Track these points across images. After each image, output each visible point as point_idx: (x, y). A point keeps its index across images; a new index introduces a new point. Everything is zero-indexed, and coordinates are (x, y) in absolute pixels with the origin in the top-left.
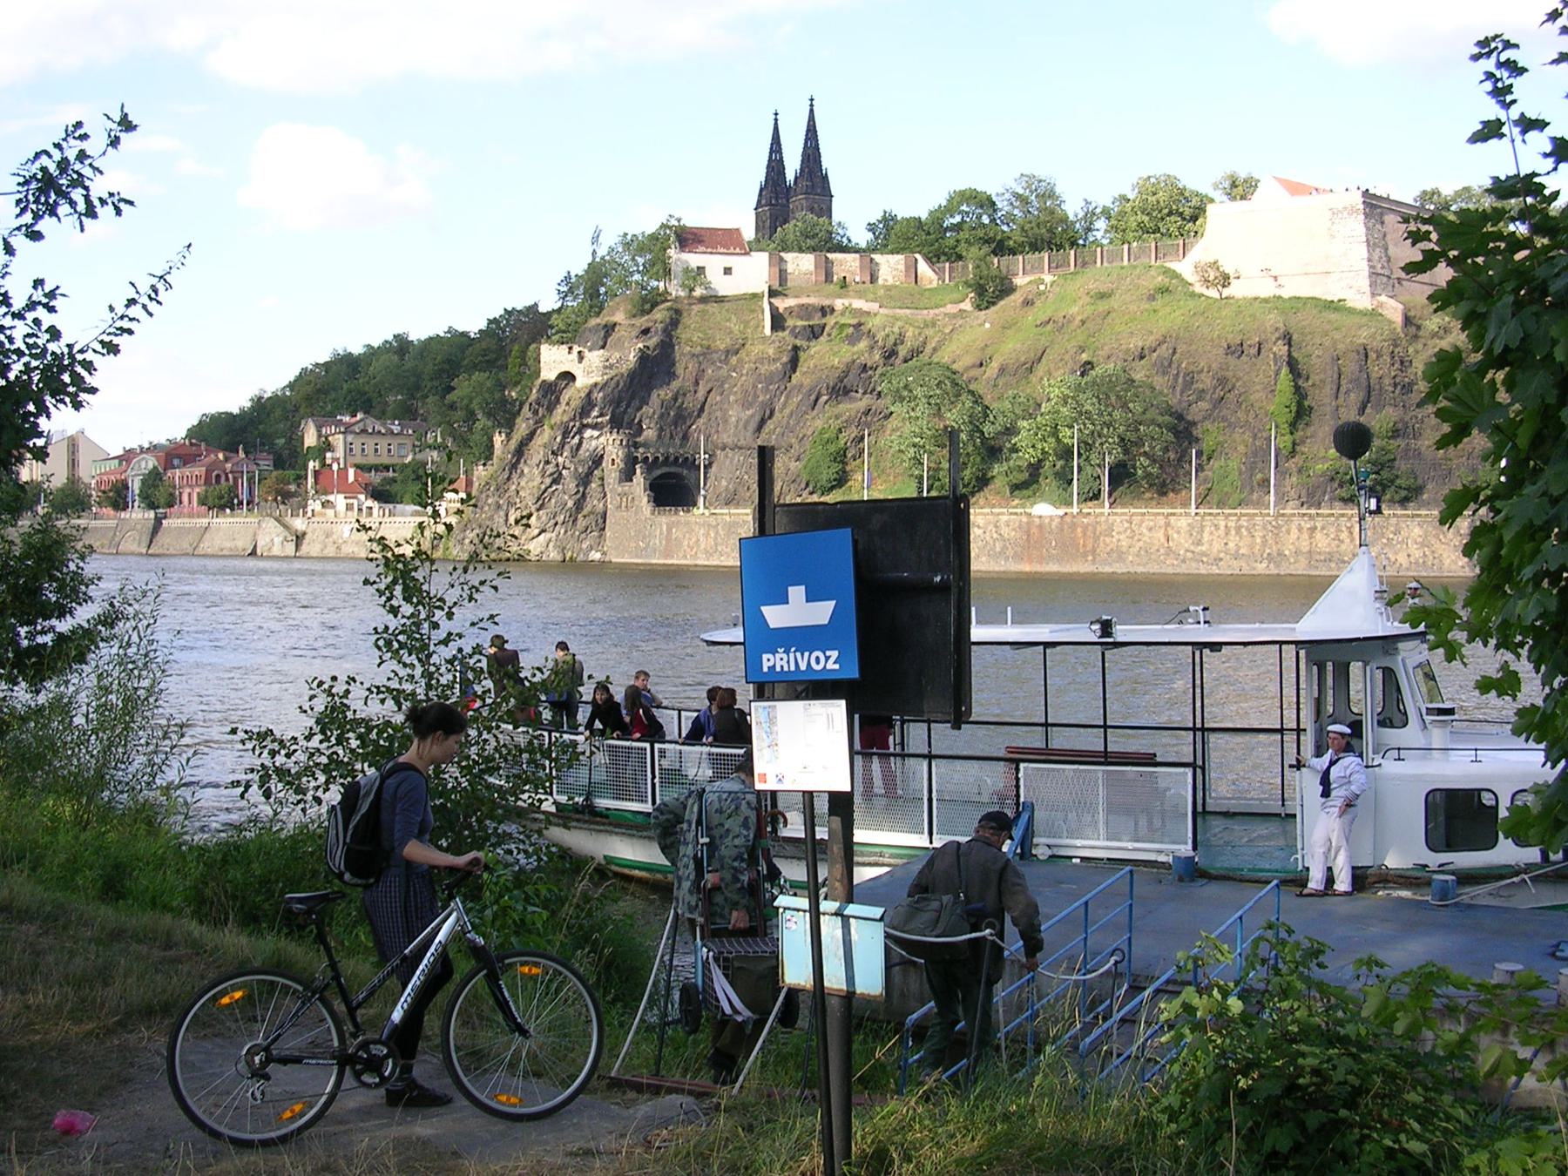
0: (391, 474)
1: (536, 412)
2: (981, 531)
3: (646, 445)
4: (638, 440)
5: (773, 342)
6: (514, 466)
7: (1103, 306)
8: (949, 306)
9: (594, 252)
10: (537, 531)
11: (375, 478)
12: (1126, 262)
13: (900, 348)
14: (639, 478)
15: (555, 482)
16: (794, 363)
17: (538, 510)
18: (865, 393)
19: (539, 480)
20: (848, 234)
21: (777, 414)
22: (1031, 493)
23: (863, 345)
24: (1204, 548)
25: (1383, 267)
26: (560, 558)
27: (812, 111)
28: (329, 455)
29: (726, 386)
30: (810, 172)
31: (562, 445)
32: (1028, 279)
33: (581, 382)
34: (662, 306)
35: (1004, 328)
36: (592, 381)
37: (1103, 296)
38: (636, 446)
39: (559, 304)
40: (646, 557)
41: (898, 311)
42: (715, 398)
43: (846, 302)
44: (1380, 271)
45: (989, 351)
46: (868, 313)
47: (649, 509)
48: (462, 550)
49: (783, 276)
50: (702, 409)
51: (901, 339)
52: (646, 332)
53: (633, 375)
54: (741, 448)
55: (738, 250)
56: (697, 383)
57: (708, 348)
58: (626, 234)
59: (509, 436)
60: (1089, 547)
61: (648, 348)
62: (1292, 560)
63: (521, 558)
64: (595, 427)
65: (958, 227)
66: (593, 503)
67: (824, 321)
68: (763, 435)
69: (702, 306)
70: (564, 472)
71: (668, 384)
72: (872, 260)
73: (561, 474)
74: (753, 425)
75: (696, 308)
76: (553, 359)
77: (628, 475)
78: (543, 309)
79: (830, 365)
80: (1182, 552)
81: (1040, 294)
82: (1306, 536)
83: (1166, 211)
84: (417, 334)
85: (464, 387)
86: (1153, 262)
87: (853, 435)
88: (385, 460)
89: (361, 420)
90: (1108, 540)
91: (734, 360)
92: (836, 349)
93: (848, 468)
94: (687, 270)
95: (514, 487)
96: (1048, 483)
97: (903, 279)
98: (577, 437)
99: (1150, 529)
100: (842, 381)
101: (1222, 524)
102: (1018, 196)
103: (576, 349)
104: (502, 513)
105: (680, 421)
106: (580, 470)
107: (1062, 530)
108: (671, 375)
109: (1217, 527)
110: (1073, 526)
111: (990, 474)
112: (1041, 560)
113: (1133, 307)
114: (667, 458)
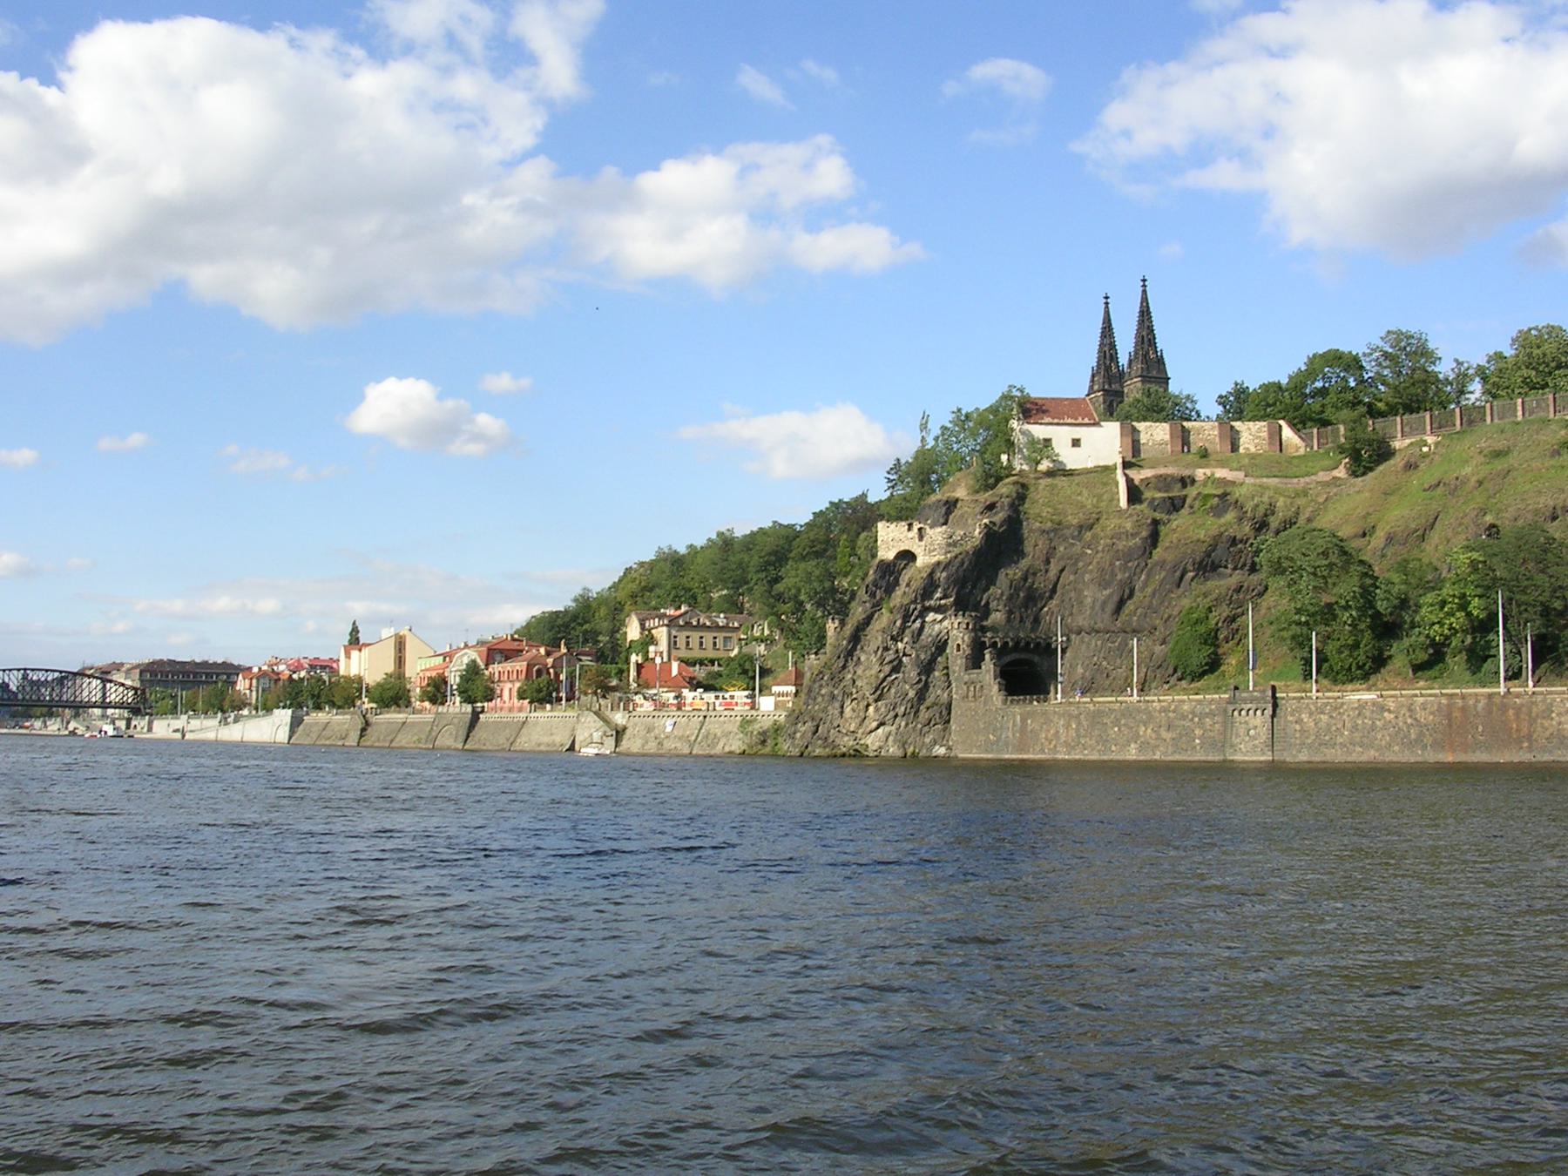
0: (716, 668)
1: (873, 595)
2: (1392, 716)
3: (993, 629)
4: (985, 623)
5: (1131, 515)
6: (850, 653)
7: (1499, 465)
8: (1321, 473)
10: (875, 724)
11: (700, 673)
12: (1520, 418)
13: (1271, 519)
14: (988, 665)
15: (896, 669)
16: (1154, 538)
18: (1235, 569)
19: (877, 668)
20: (1198, 407)
21: (1137, 593)
22: (1437, 674)
23: (1230, 516)
26: (900, 753)
28: (652, 648)
29: (1081, 564)
31: (903, 630)
32: (1408, 441)
33: (921, 561)
34: (1007, 480)
35: (1385, 494)
36: (935, 560)
37: (1498, 454)
38: (984, 630)
39: (888, 493)
40: (999, 751)
41: (1265, 480)
42: (1068, 577)
43: (1208, 472)
45: (1371, 521)
46: (1233, 483)
47: (1000, 698)
48: (793, 744)
49: (1136, 447)
50: (1054, 591)
51: (1271, 510)
52: (991, 507)
53: (979, 553)
54: (1098, 632)
55: (1086, 421)
56: (1048, 562)
57: (1060, 523)
58: (959, 410)
59: (843, 623)
61: (994, 524)
63: (857, 754)
64: (938, 610)
65: (1323, 392)
66: (937, 693)
67: (1184, 493)
68: (1123, 617)
69: (1049, 481)
70: (904, 659)
71: (1016, 563)
72: (1232, 427)
73: (901, 661)
74: (1111, 607)
75: (1044, 482)
77: (975, 661)
78: (871, 499)
79: (1195, 538)
81: (1425, 456)
83: (1553, 364)
84: (741, 531)
85: (793, 577)
86: (1551, 416)
87: (1225, 615)
88: (711, 654)
89: (686, 613)
91: (1088, 536)
92: (1200, 521)
93: (1220, 651)
94: (1033, 442)
95: (849, 676)
96: (1456, 663)
97: (1266, 447)
98: (919, 621)
100: (1209, 556)
102: (1386, 355)
103: (916, 526)
104: (837, 705)
105: (1031, 604)
106: (923, 657)
108: (1021, 554)
111: (1387, 654)
113: (1536, 464)
114: (1017, 644)
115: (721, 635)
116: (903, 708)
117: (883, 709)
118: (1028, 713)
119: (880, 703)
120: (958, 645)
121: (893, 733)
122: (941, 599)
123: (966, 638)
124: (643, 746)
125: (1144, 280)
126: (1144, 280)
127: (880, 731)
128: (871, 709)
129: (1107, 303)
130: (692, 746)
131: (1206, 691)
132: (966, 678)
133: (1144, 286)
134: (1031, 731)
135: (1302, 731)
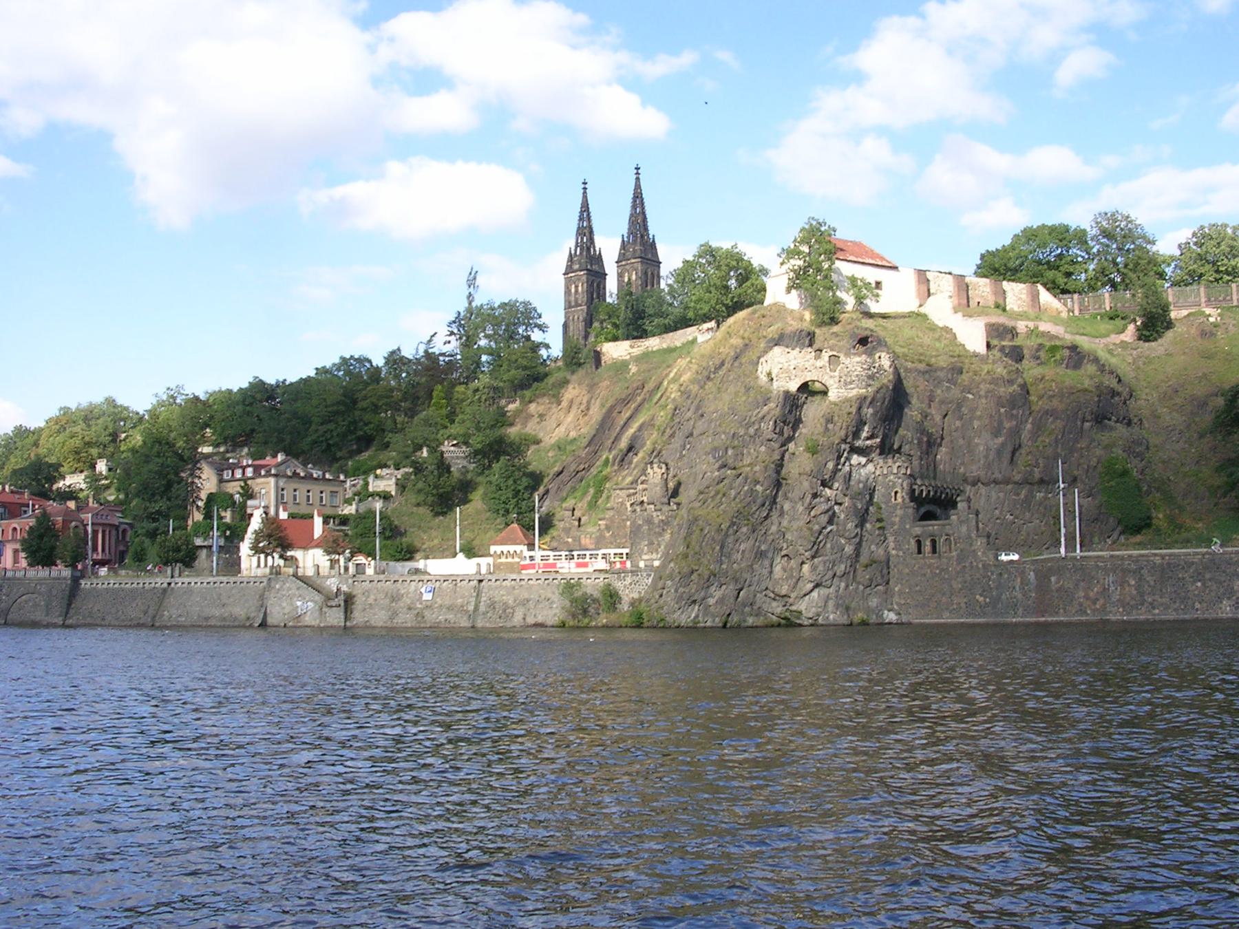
10: (810, 586)
17: (813, 557)
33: (833, 395)
66: (872, 549)
98: (847, 464)
115: (328, 489)
116: (843, 567)
117: (821, 568)
118: (1050, 569)
119: (816, 560)
120: (896, 493)
121: (832, 596)
123: (905, 485)
124: (391, 619)
125: (637, 169)
126: (637, 169)
127: (815, 594)
128: (806, 567)
129: (585, 189)
131: (1141, 545)
132: (918, 530)
134: (1058, 590)
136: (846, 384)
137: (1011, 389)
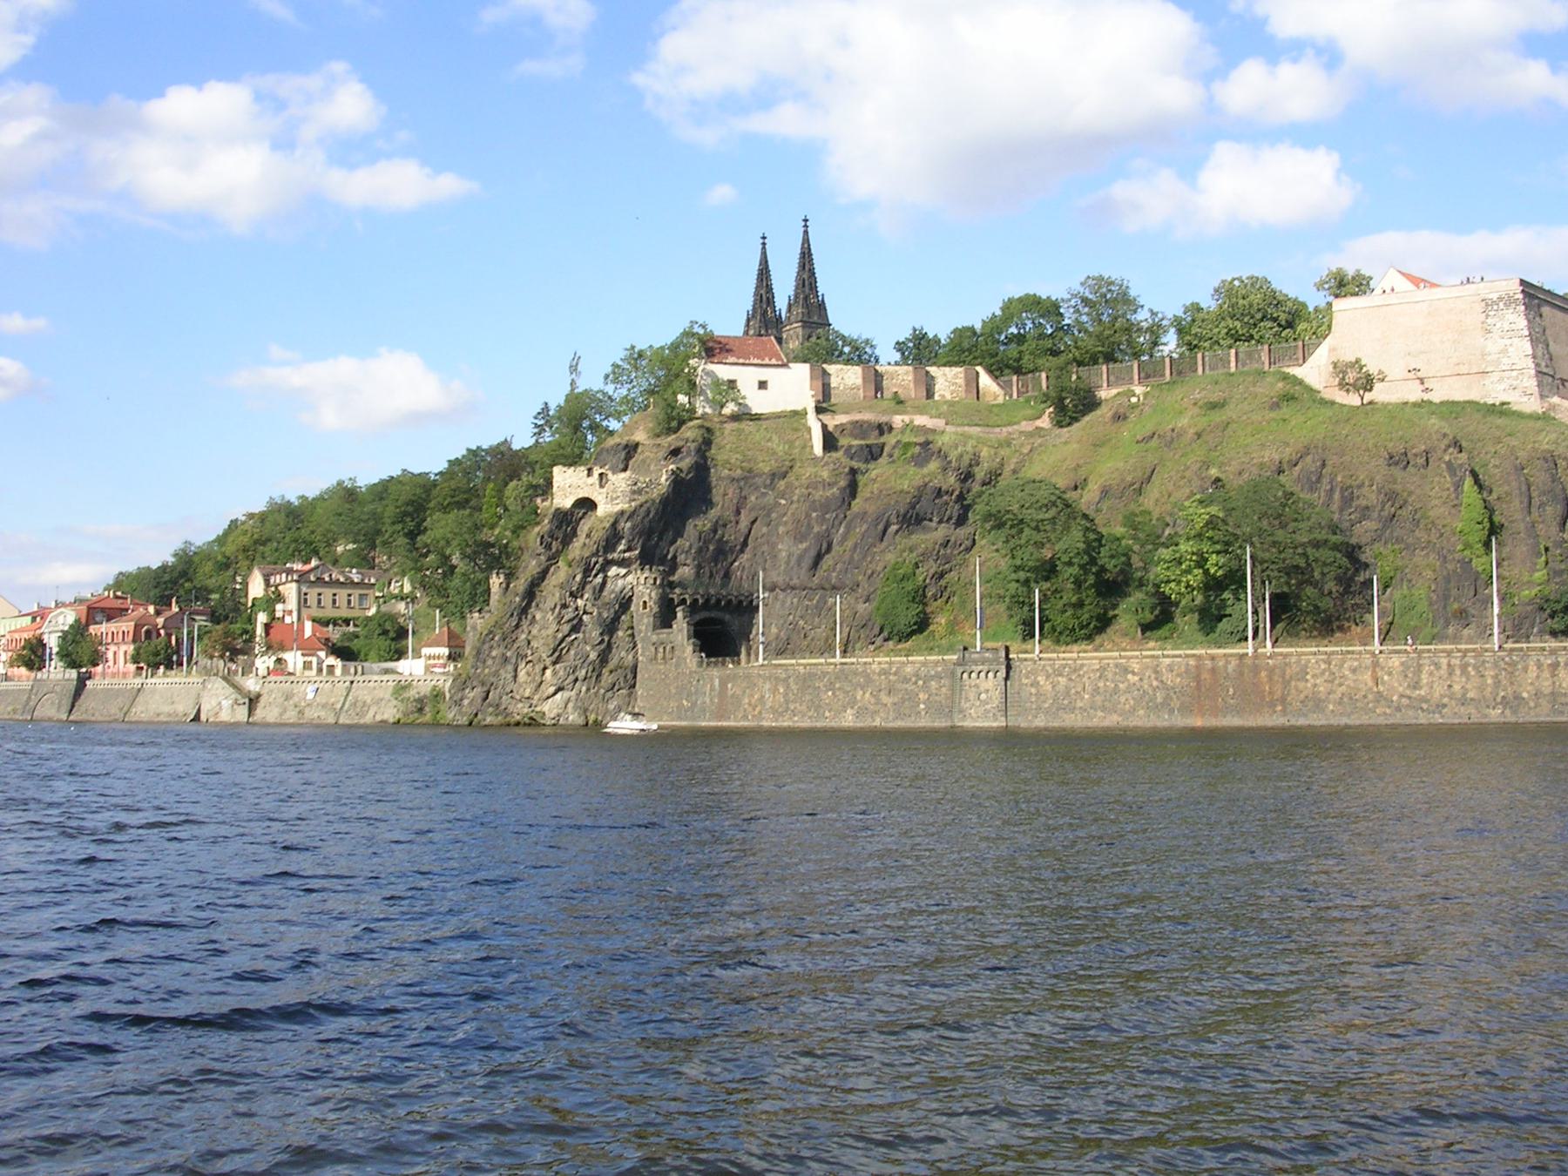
0: (351, 628)
1: (549, 547)
3: (681, 584)
4: (671, 579)
5: (827, 464)
6: (524, 611)
7: (1218, 417)
8: (1024, 423)
9: (573, 383)
10: (552, 689)
11: (334, 634)
12: (1233, 369)
13: (976, 469)
14: (681, 623)
15: (575, 629)
16: (852, 489)
17: (554, 663)
18: (940, 522)
19: (554, 627)
20: (877, 352)
21: (835, 547)
22: (1168, 634)
23: (934, 465)
24: (1423, 693)
25: (1547, 366)
26: (581, 721)
27: (806, 232)
28: (279, 607)
29: (774, 515)
30: (806, 298)
31: (583, 584)
32: (1114, 391)
33: (602, 510)
34: (691, 424)
35: (1095, 445)
36: (617, 508)
37: (1213, 406)
38: (672, 585)
39: (532, 441)
40: (694, 719)
41: (966, 428)
42: (760, 529)
43: (907, 418)
44: (1545, 370)
45: (1082, 473)
46: (933, 431)
47: (695, 660)
48: (460, 712)
49: (826, 391)
50: (745, 544)
51: (976, 461)
52: (675, 452)
53: (666, 501)
54: (793, 588)
55: (774, 361)
56: (738, 512)
57: (750, 471)
58: (633, 347)
59: (510, 577)
60: (1278, 694)
61: (681, 471)
62: (1532, 704)
63: (533, 722)
64: (622, 563)
65: (1020, 339)
66: (620, 655)
67: (882, 440)
68: (820, 573)
69: (735, 425)
70: (585, 617)
71: (705, 513)
72: (927, 372)
73: (581, 619)
74: (808, 562)
75: (729, 426)
76: (569, 485)
77: (665, 618)
78: (516, 446)
79: (899, 488)
80: (1395, 698)
81: (1133, 407)
82: (1546, 674)
83: (1259, 316)
84: (367, 477)
85: (440, 526)
86: (1266, 368)
87: (932, 571)
88: (344, 613)
89: (317, 567)
90: (1301, 685)
91: (782, 484)
92: (901, 471)
93: (928, 610)
94: (717, 383)
95: (523, 636)
96: (1186, 623)
97: (963, 395)
98: (601, 575)
99: (1354, 671)
100: (913, 507)
101: (1444, 661)
102: (1085, 301)
103: (597, 471)
104: (510, 668)
105: (721, 557)
106: (605, 615)
107: (1241, 674)
108: (709, 504)
109: (1437, 666)
110: (1256, 670)
111: (1111, 613)
112: (1215, 712)
113: (1256, 417)
114: (707, 601)
115: (356, 592)
116: (584, 672)
117: (561, 673)
118: (728, 676)
119: (558, 666)
120: (645, 602)
121: (573, 698)
122: (625, 552)
123: (653, 594)
124: (281, 715)
127: (559, 696)
128: (548, 672)
129: (764, 244)
130: (338, 715)
131: (919, 652)
132: (654, 638)
133: (806, 226)
135: (1038, 694)
136: (612, 499)
137: (828, 494)
